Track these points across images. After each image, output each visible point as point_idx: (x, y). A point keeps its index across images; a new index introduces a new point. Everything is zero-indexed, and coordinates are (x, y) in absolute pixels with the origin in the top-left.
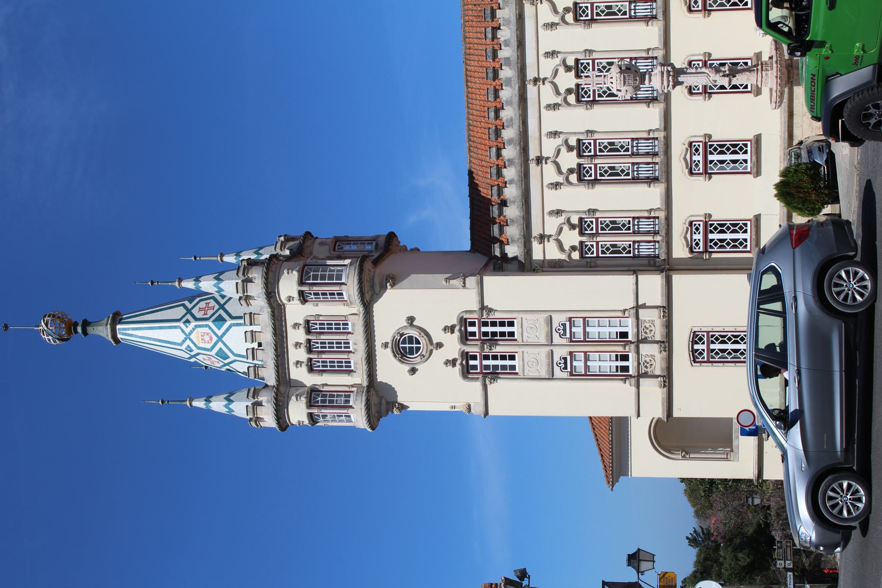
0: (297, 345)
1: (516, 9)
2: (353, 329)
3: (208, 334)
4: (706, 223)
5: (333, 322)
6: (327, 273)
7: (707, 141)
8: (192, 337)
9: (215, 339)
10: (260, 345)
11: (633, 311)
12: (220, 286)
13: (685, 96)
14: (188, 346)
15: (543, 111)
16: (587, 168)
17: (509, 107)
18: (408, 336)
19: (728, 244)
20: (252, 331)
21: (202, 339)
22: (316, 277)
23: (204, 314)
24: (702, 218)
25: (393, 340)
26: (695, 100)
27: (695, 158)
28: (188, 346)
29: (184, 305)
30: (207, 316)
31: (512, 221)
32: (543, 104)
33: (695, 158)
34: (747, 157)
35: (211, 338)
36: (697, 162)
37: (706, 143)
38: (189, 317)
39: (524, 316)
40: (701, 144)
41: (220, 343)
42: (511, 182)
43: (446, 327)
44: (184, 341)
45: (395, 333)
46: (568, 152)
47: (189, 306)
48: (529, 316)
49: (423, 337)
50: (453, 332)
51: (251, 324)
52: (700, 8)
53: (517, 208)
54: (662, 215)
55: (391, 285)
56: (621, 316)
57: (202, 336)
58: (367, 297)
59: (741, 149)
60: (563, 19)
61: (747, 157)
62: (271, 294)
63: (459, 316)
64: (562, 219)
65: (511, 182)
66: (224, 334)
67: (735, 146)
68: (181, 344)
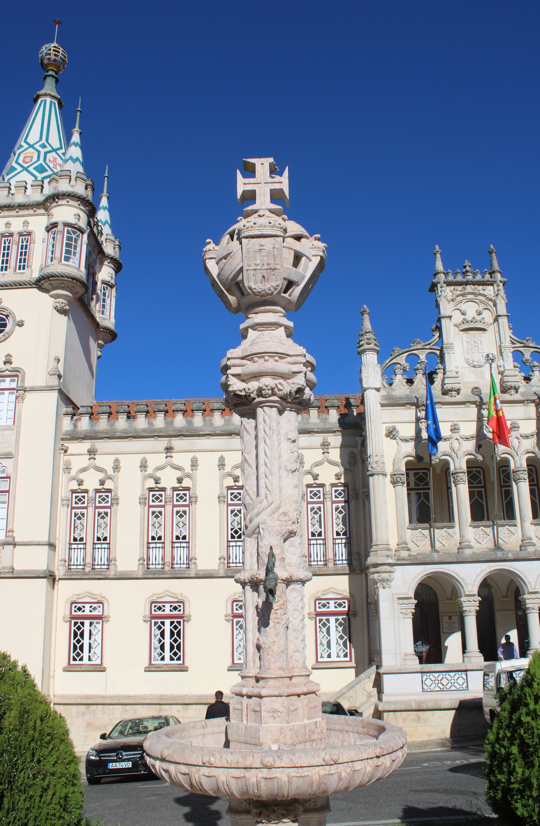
0: (8, 224)
1: (318, 429)
2: (18, 273)
3: (31, 160)
4: (99, 618)
5: (27, 257)
6: (73, 250)
7: (184, 619)
8: (31, 150)
9: (26, 165)
10: (12, 194)
11: (11, 539)
12: (70, 161)
13: (231, 596)
14: (23, 146)
15: (219, 454)
16: (161, 498)
17: (223, 422)
18: (6, 324)
19: (78, 641)
20: (26, 188)
21: (27, 157)
22: (70, 239)
23: (50, 161)
24: (106, 614)
25: (4, 309)
26: (226, 606)
27: (167, 606)
28: (23, 146)
29: (61, 148)
30: (47, 161)
31: (112, 425)
32: (225, 454)
33: (167, 606)
34: (167, 660)
35: (26, 163)
36: (163, 608)
37: (182, 617)
38: (49, 149)
39: (15, 432)
40: (181, 612)
41: (21, 169)
42: (151, 424)
43: (12, 357)
44: (27, 143)
45: (10, 310)
46: (178, 478)
47: (60, 152)
48: (14, 437)
49: (4, 336)
50: (5, 363)
51: (32, 186)
52: (318, 610)
53: (125, 429)
54: (111, 573)
55: (57, 307)
56: (8, 529)
57: (30, 157)
58: (46, 285)
59: (175, 654)
60: (309, 473)
61: (167, 660)
62: (55, 197)
63: (21, 369)
64: (110, 472)
65: (151, 424)
66: (29, 172)
67: (179, 647)
68: (25, 142)
